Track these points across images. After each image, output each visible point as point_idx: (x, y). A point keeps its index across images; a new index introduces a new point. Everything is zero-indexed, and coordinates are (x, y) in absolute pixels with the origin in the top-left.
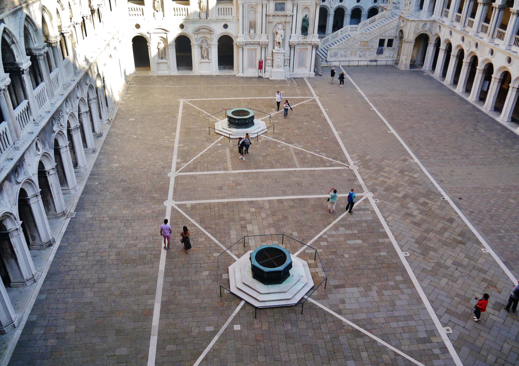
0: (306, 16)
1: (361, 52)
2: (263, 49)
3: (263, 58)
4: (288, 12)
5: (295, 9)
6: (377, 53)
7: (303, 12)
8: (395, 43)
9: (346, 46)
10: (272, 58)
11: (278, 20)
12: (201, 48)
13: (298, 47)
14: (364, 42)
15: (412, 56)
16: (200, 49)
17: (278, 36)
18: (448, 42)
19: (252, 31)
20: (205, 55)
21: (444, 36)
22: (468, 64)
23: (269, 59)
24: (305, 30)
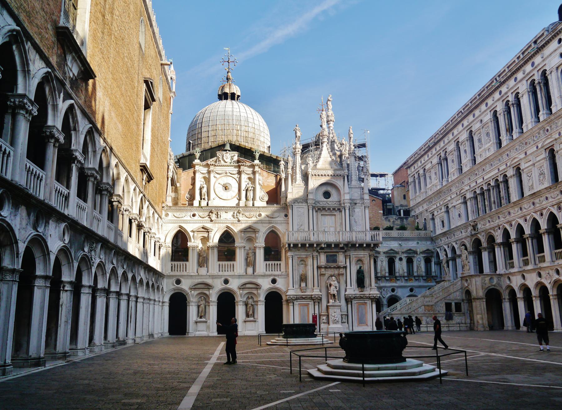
0: (360, 267)
1: (427, 317)
2: (317, 304)
3: (317, 312)
4: (342, 264)
5: (348, 260)
6: (446, 319)
7: (356, 264)
8: (464, 307)
9: (409, 311)
10: (327, 314)
11: (329, 272)
12: (246, 305)
13: (355, 302)
14: (428, 306)
15: (488, 321)
16: (244, 307)
17: (332, 287)
18: (523, 288)
19: (303, 285)
20: (251, 312)
21: (516, 282)
22: (556, 297)
23: (324, 315)
24: (361, 283)
